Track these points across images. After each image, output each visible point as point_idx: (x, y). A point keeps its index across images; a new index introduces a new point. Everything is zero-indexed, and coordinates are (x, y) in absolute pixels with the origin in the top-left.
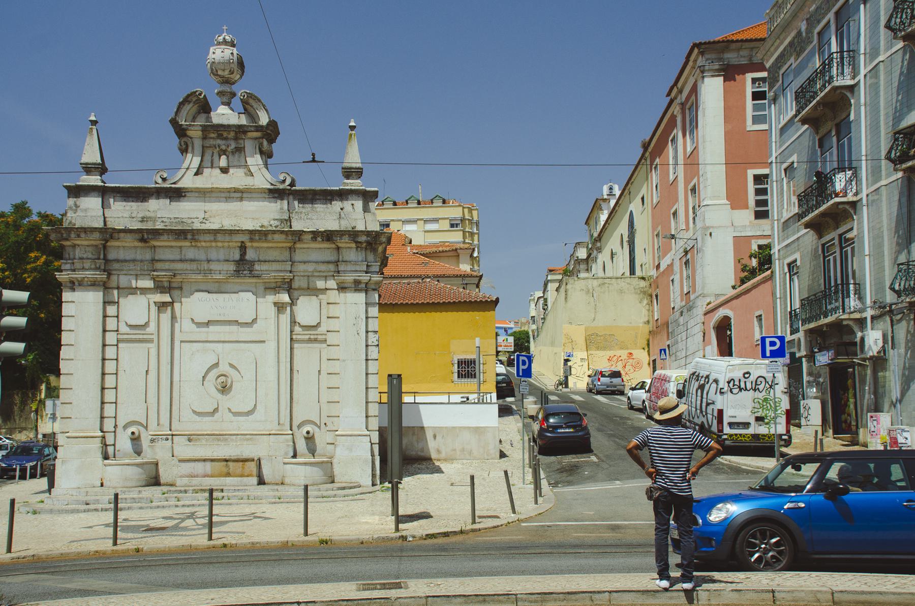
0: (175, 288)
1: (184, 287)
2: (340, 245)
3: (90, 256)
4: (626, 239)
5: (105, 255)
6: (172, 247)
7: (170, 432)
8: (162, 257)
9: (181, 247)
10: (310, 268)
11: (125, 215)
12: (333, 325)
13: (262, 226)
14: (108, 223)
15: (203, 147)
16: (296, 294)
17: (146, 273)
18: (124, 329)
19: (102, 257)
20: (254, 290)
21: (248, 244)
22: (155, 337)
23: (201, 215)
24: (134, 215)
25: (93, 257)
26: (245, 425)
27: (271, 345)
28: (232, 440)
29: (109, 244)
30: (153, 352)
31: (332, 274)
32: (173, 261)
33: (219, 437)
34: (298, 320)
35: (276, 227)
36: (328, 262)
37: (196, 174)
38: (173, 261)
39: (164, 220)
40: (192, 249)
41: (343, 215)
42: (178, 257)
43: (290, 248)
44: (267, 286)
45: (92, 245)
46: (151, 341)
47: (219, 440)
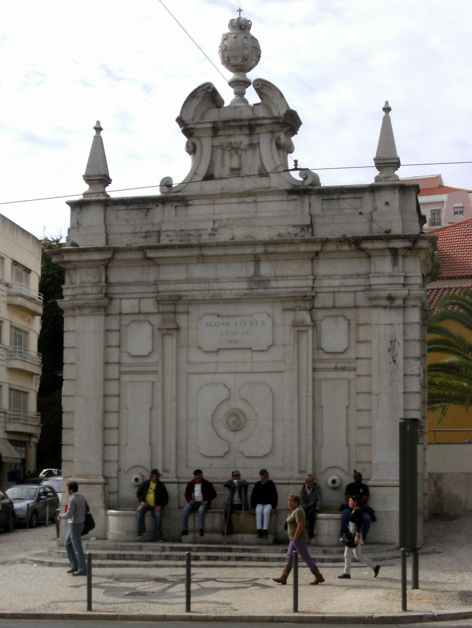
0: (181, 313)
3: (92, 279)
5: (107, 278)
11: (128, 231)
12: (363, 351)
13: (279, 235)
14: (111, 241)
15: (213, 147)
16: (319, 314)
17: (150, 295)
18: (126, 359)
19: (103, 279)
20: (270, 311)
22: (159, 369)
23: (210, 225)
24: (137, 230)
31: (363, 288)
34: (324, 345)
35: (296, 235)
38: (178, 282)
39: (169, 233)
41: (375, 217)
46: (155, 372)
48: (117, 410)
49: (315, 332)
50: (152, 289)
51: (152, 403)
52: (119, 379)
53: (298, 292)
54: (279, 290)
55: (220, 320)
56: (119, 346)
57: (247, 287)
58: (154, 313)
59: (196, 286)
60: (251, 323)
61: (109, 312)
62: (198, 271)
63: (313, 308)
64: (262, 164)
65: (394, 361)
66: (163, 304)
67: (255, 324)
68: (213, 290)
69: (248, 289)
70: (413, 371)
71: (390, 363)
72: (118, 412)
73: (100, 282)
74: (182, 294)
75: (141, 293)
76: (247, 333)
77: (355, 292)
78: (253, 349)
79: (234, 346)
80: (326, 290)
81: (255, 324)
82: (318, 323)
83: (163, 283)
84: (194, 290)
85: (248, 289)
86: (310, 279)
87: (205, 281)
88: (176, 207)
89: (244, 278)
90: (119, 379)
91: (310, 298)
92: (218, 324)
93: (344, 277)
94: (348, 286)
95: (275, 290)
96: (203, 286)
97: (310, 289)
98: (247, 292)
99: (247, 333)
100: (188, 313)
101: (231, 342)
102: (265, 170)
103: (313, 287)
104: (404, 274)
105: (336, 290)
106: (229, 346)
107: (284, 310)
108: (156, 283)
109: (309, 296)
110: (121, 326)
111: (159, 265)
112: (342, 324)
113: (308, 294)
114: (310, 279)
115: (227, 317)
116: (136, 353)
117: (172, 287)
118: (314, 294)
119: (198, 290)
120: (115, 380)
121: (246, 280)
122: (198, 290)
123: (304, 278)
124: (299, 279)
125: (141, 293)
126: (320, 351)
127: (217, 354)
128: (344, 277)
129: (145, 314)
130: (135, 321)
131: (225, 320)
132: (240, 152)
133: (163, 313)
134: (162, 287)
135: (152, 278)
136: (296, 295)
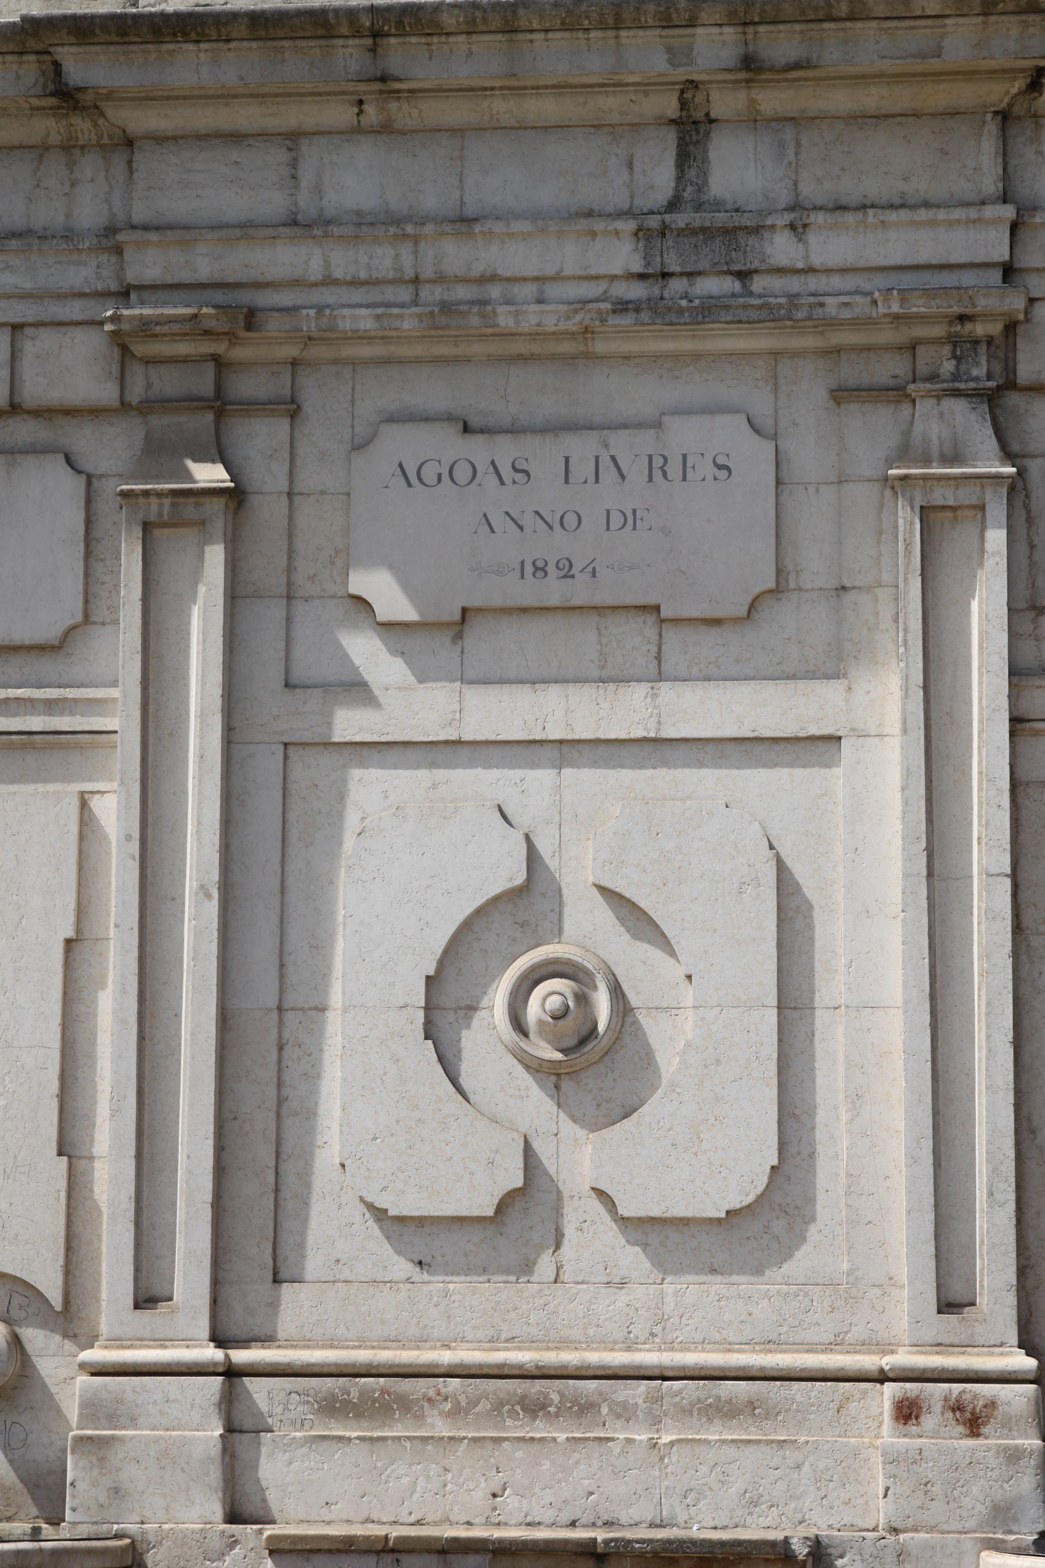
0: (254, 407)
1: (311, 400)
6: (234, 138)
7: (212, 1354)
8: (175, 205)
9: (292, 139)
17: (75, 310)
20: (761, 403)
21: (724, 103)
26: (710, 1318)
27: (884, 768)
28: (625, 1413)
30: (114, 811)
32: (245, 230)
33: (539, 1391)
38: (245, 230)
40: (366, 154)
42: (274, 203)
43: (1005, 117)
44: (852, 372)
47: (535, 1409)
49: (1021, 515)
50: (84, 273)
51: (81, 912)
53: (929, 293)
54: (813, 283)
55: (478, 449)
57: (637, 267)
58: (95, 412)
59: (344, 261)
60: (656, 469)
62: (355, 178)
63: (1011, 385)
66: (149, 361)
67: (674, 469)
68: (441, 279)
69: (642, 277)
74: (263, 299)
75: (23, 296)
76: (632, 519)
78: (665, 613)
79: (553, 591)
81: (674, 469)
83: (153, 236)
84: (329, 281)
85: (642, 277)
86: (996, 221)
87: (394, 224)
89: (620, 215)
91: (995, 329)
92: (463, 473)
95: (794, 284)
96: (383, 258)
97: (995, 277)
98: (637, 291)
99: (632, 519)
100: (292, 409)
101: (541, 570)
103: (1009, 271)
106: (525, 591)
107: (842, 395)
108: (111, 238)
109: (987, 316)
111: (129, 143)
113: (983, 303)
114: (996, 221)
115: (514, 430)
117: (204, 264)
118: (1016, 303)
119: (354, 283)
121: (630, 225)
122: (354, 283)
123: (958, 214)
124: (932, 223)
125: (23, 296)
127: (459, 636)
129: (44, 413)
131: (505, 451)
133: (147, 407)
134: (148, 264)
135: (89, 211)
136: (918, 307)
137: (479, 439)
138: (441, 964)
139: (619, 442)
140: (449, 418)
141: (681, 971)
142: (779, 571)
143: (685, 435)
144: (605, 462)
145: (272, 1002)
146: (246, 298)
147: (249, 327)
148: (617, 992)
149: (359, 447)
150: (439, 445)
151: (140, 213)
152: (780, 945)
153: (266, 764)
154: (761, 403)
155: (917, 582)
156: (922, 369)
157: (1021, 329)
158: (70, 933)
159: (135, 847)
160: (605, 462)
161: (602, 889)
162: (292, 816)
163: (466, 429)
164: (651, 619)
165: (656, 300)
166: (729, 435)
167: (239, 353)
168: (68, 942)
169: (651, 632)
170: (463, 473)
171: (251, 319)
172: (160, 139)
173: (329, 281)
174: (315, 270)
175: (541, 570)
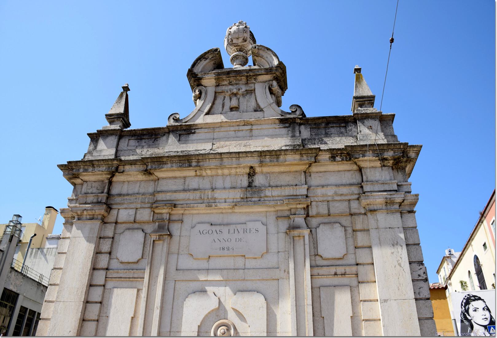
1: (185, 220)
2: (362, 164)
4: (473, 272)
5: (109, 190)
6: (175, 178)
8: (164, 188)
9: (185, 178)
10: (330, 191)
15: (216, 93)
19: (106, 191)
21: (258, 170)
25: (98, 191)
29: (114, 179)
32: (175, 191)
34: (320, 252)
36: (351, 185)
37: (208, 114)
38: (175, 191)
40: (197, 179)
42: (181, 188)
44: (280, 214)
45: (99, 181)
48: (96, 319)
52: (104, 286)
55: (214, 228)
56: (110, 253)
60: (245, 231)
61: (106, 220)
64: (258, 104)
65: (400, 265)
67: (248, 231)
70: (419, 275)
71: (395, 266)
72: (97, 321)
73: (102, 193)
74: (177, 203)
77: (349, 200)
80: (321, 199)
81: (248, 231)
82: (313, 230)
88: (180, 135)
90: (104, 286)
92: (210, 232)
93: (337, 186)
94: (342, 195)
97: (305, 197)
99: (240, 240)
100: (182, 221)
101: (223, 249)
102: (259, 107)
104: (396, 181)
105: (330, 199)
108: (153, 194)
110: (115, 233)
112: (339, 231)
116: (124, 259)
120: (100, 286)
126: (318, 258)
127: (208, 261)
128: (337, 186)
130: (129, 229)
131: (218, 228)
132: (238, 96)
137: (213, 226)
138: (201, 323)
139: (239, 227)
140: (208, 223)
141: (248, 325)
142: (267, 248)
143: (250, 225)
144: (236, 230)
145: (168, 330)
146: (174, 202)
147: (175, 207)
148: (235, 328)
149: (193, 228)
150: (207, 227)
151: (159, 189)
152: (267, 320)
153: (171, 285)
154: (264, 220)
155: (292, 249)
156: (292, 213)
157: (310, 207)
158: (133, 316)
159: (145, 299)
160: (236, 230)
161: (233, 309)
162: (175, 294)
163: (211, 225)
164: (243, 258)
165: (245, 200)
166: (259, 225)
167: (173, 212)
168: (132, 317)
169: (243, 260)
170: (210, 232)
171: (175, 206)
172: (163, 178)
173: (189, 199)
174: (187, 197)
175: (223, 249)
